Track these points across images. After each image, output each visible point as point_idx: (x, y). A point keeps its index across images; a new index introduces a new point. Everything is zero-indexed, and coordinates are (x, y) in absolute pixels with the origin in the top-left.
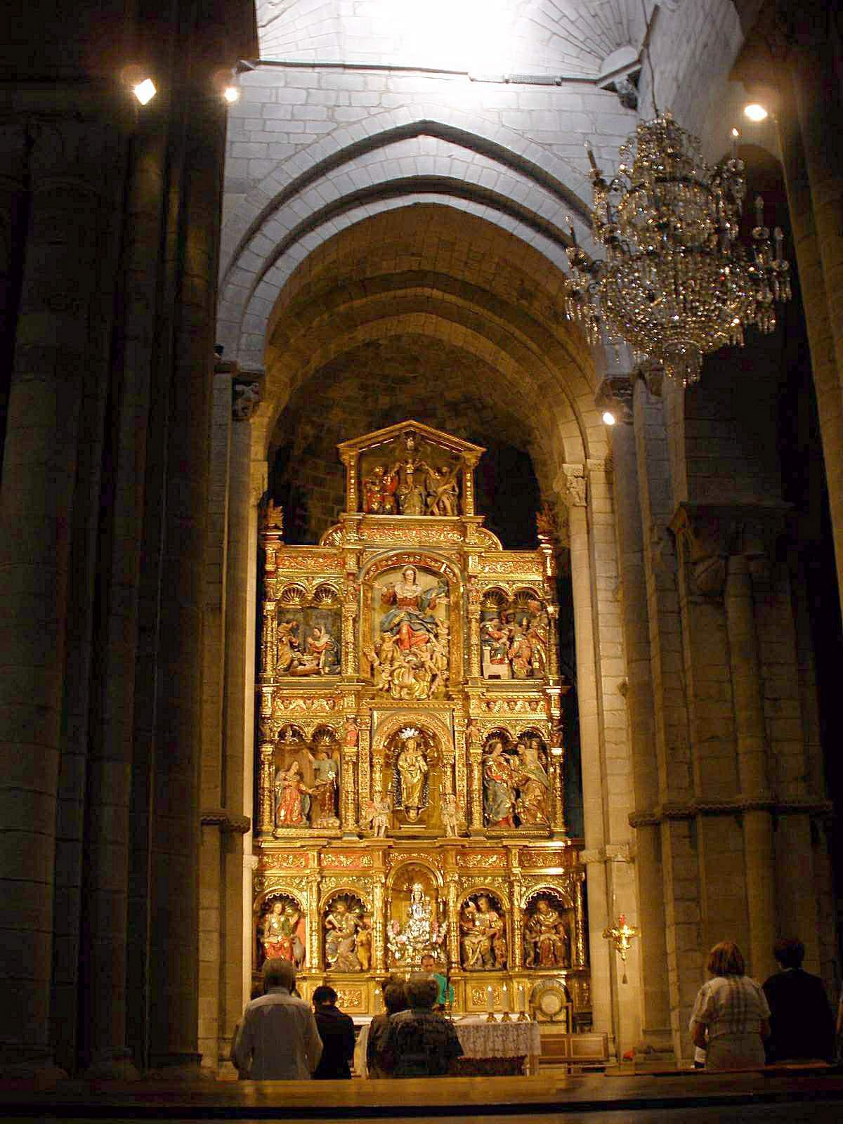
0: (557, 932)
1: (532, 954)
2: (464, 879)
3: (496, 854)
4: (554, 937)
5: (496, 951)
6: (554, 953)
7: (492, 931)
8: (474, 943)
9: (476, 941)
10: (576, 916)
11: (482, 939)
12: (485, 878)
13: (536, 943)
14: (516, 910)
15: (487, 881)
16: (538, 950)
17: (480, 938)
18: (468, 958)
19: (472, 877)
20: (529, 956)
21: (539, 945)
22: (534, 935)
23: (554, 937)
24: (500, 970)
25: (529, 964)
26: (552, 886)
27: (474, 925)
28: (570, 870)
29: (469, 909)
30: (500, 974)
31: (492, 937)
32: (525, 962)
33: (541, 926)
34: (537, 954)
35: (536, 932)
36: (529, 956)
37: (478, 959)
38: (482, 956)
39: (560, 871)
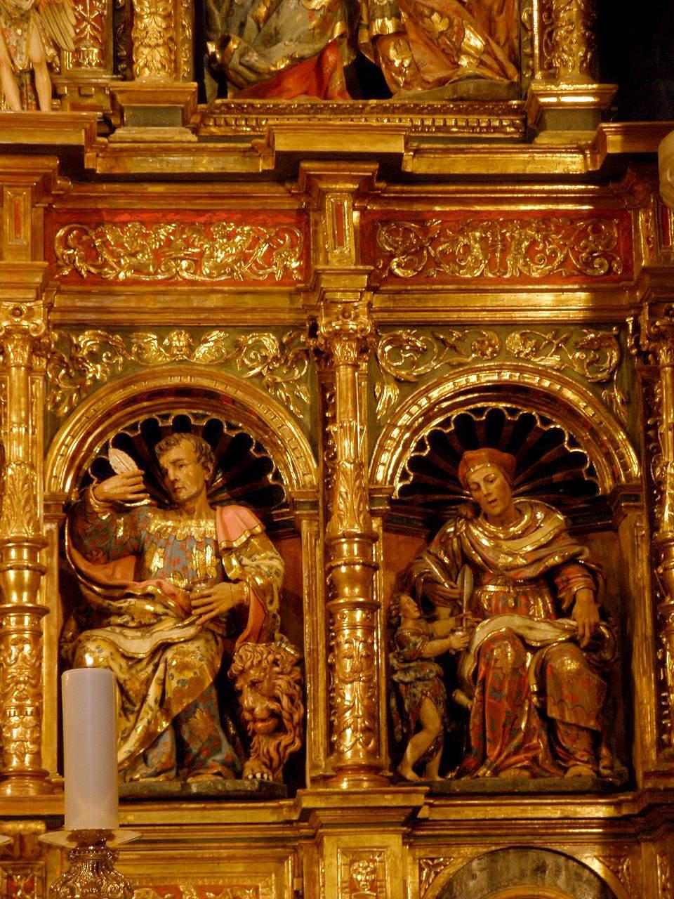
0: (560, 611)
1: (432, 714)
2: (86, 341)
3: (245, 217)
4: (544, 631)
5: (248, 700)
6: (542, 711)
7: (225, 597)
8: (132, 660)
9: (140, 646)
11: (176, 635)
12: (197, 333)
13: (449, 661)
14: (346, 498)
15: (202, 351)
16: (461, 697)
17: (168, 630)
19: (128, 330)
20: (420, 727)
21: (468, 666)
22: (441, 626)
23: (544, 631)
24: (264, 794)
25: (420, 767)
28: (625, 299)
29: (110, 487)
30: (263, 814)
31: (235, 620)
32: (397, 751)
33: (478, 584)
34: (455, 715)
35: (455, 604)
36: (420, 727)
37: (151, 740)
39: (576, 302)
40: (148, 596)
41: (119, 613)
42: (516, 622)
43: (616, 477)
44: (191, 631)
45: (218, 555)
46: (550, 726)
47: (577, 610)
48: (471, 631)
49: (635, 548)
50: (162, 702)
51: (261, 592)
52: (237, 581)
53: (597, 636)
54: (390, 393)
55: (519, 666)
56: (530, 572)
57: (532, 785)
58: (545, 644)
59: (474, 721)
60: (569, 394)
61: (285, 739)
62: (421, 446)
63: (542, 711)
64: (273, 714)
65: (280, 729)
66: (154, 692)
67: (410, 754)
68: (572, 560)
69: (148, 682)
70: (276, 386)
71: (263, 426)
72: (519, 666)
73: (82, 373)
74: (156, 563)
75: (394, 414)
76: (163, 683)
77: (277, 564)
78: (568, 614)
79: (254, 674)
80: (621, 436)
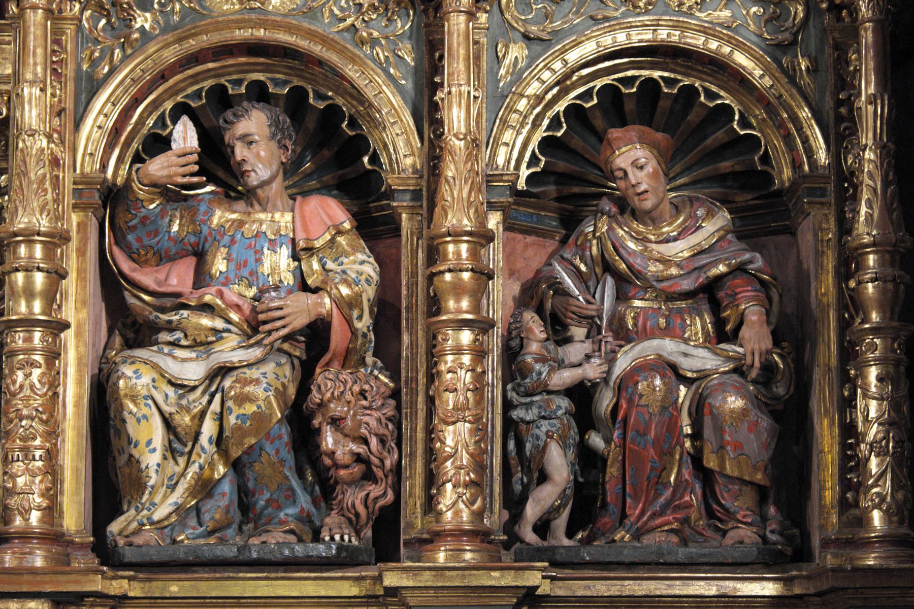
5: (329, 440)
6: (697, 459)
10: (845, 227)
16: (596, 440)
18: (139, 484)
20: (544, 478)
21: (605, 401)
22: (575, 351)
25: (543, 527)
26: (697, 41)
27: (201, 278)
36: (544, 478)
38: (236, 466)
40: (207, 308)
41: (170, 327)
42: (668, 347)
43: (796, 165)
44: (256, 353)
45: (295, 257)
46: (706, 476)
47: (745, 332)
48: (611, 361)
49: (819, 255)
50: (220, 441)
51: (348, 305)
52: (316, 291)
53: (768, 368)
54: (517, 52)
55: (670, 404)
56: (687, 285)
57: (682, 554)
58: (703, 375)
59: (613, 471)
60: (741, 59)
61: (375, 490)
62: (555, 123)
63: (697, 459)
64: (359, 458)
65: (369, 476)
66: (209, 428)
67: (532, 511)
68: (740, 269)
69: (202, 414)
70: (374, 42)
71: (357, 96)
72: (670, 404)
73: (128, 22)
74: (220, 265)
75: (518, 77)
76: (221, 418)
77: (371, 270)
78: (733, 337)
79: (337, 409)
80: (805, 113)
